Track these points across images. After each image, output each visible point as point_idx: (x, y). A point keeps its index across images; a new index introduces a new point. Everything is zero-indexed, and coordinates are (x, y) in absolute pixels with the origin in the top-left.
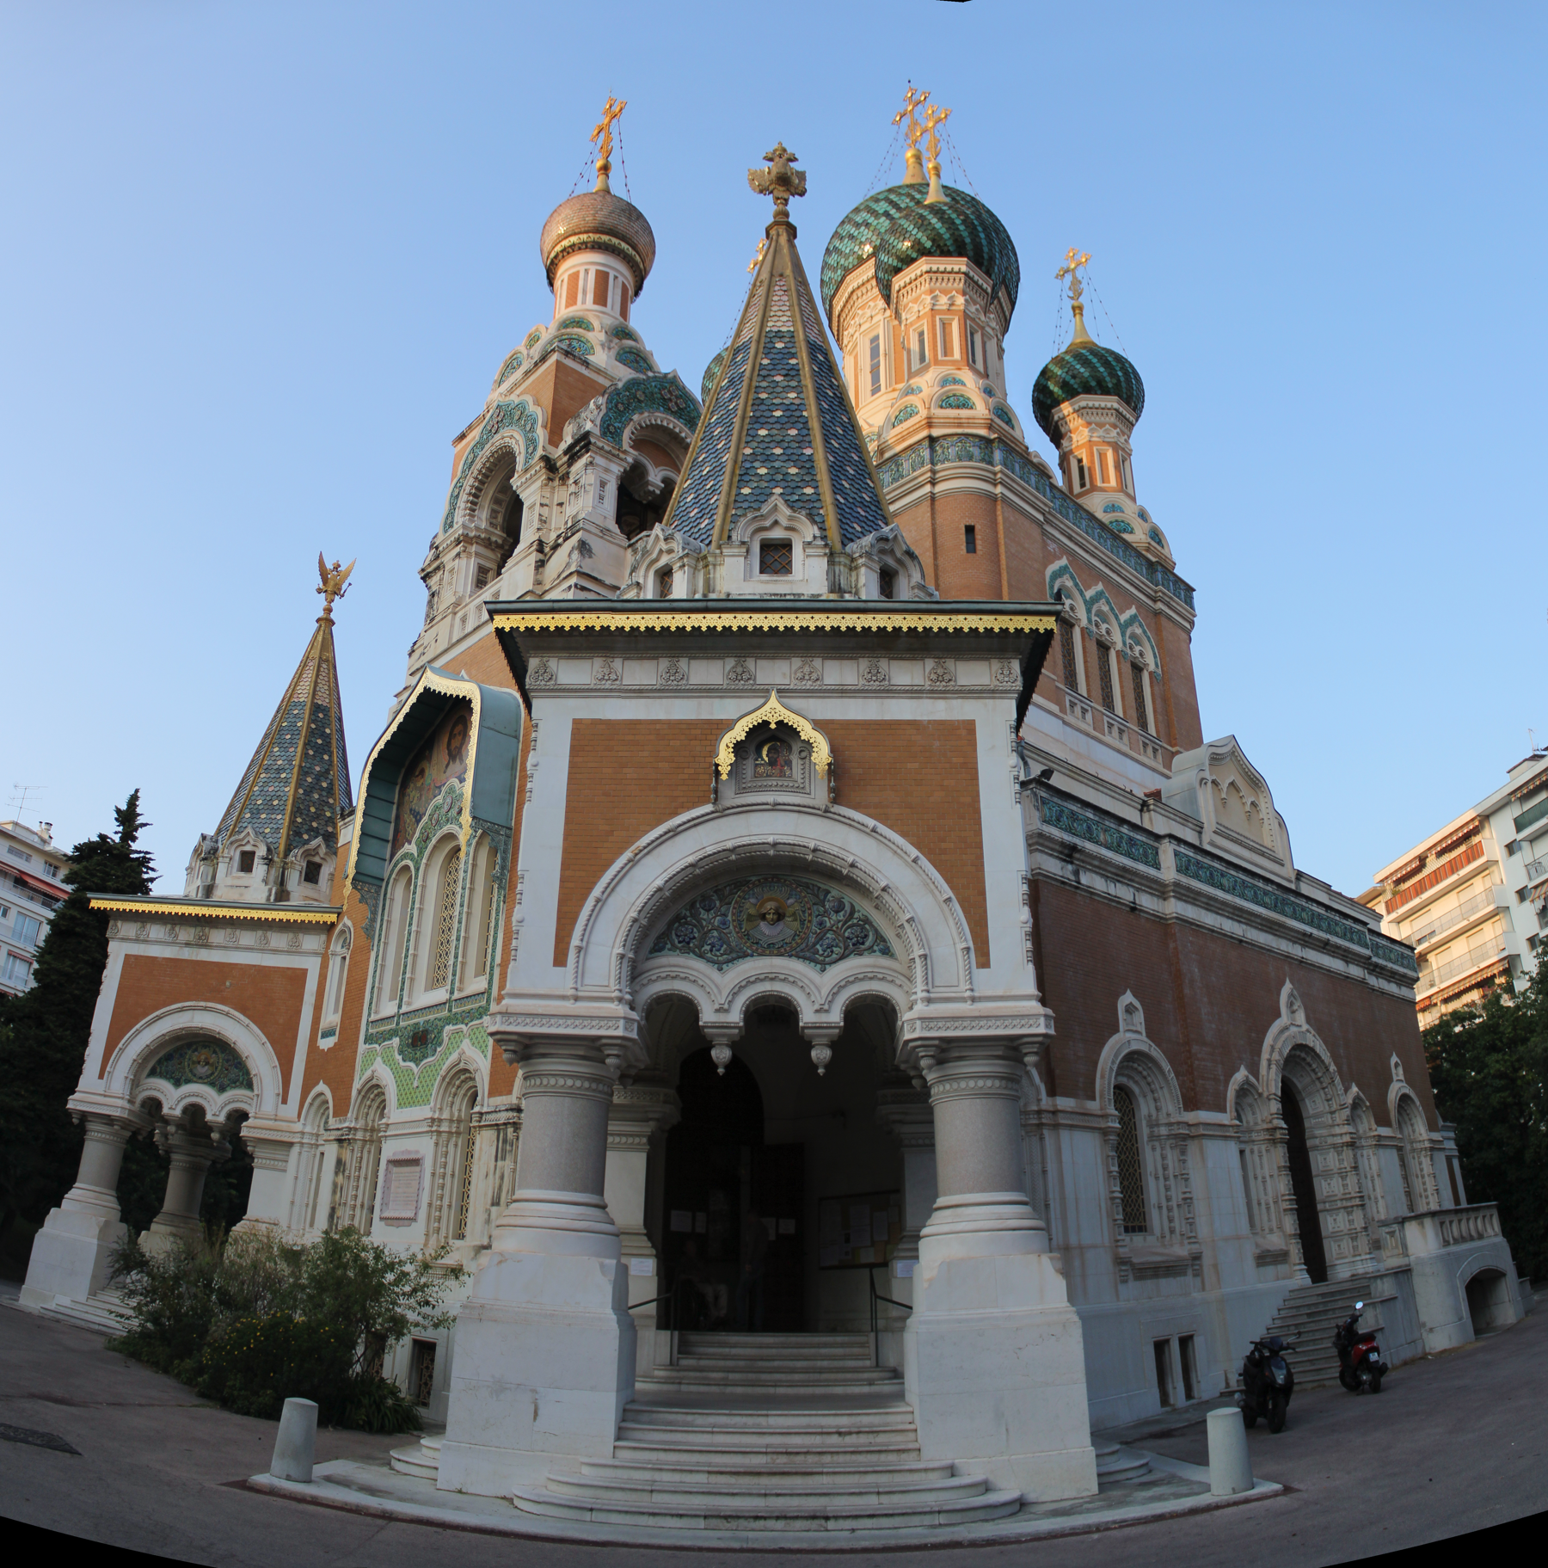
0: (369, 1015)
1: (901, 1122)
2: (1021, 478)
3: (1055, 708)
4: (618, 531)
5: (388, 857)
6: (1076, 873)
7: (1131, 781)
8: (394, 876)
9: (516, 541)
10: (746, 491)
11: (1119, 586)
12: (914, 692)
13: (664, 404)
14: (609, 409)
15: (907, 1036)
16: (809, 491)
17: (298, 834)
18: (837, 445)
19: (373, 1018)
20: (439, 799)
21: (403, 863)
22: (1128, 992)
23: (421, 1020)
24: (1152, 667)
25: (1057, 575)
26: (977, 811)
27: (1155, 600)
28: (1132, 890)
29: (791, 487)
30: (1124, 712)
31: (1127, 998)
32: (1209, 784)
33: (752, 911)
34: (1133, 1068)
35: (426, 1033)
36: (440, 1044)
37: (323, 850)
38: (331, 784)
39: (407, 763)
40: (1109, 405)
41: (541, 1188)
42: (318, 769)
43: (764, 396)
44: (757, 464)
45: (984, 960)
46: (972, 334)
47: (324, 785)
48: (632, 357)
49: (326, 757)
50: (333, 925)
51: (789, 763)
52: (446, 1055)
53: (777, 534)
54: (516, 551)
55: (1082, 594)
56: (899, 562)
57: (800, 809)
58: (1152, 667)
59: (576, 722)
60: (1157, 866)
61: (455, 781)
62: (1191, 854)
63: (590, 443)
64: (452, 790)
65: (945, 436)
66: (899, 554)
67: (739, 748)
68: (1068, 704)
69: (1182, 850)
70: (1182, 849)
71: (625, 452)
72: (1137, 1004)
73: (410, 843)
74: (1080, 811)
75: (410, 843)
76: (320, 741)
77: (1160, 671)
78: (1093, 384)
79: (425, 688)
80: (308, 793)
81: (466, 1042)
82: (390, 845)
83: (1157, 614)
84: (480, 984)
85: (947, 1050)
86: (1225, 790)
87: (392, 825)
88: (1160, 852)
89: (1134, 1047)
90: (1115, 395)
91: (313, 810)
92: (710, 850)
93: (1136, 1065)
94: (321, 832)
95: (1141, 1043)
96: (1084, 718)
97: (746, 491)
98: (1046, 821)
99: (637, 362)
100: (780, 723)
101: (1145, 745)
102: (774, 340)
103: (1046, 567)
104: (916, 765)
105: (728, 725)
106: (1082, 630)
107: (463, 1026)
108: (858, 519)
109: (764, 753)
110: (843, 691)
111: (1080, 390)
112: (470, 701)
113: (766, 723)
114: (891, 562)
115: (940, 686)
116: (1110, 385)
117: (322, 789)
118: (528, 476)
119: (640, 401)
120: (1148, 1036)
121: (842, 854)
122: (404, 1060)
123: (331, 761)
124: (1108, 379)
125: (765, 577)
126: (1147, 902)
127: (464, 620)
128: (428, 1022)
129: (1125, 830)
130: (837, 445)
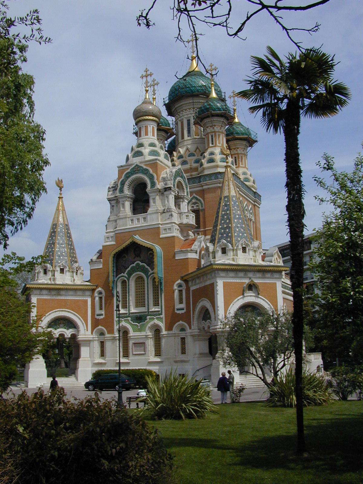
8: (119, 280)
20: (134, 265)
24: (253, 220)
27: (254, 202)
29: (243, 234)
42: (70, 243)
43: (234, 212)
49: (71, 239)
51: (252, 289)
58: (253, 220)
61: (140, 262)
73: (124, 273)
75: (124, 273)
79: (133, 241)
83: (255, 205)
97: (236, 234)
117: (72, 249)
125: (243, 254)
128: (141, 315)
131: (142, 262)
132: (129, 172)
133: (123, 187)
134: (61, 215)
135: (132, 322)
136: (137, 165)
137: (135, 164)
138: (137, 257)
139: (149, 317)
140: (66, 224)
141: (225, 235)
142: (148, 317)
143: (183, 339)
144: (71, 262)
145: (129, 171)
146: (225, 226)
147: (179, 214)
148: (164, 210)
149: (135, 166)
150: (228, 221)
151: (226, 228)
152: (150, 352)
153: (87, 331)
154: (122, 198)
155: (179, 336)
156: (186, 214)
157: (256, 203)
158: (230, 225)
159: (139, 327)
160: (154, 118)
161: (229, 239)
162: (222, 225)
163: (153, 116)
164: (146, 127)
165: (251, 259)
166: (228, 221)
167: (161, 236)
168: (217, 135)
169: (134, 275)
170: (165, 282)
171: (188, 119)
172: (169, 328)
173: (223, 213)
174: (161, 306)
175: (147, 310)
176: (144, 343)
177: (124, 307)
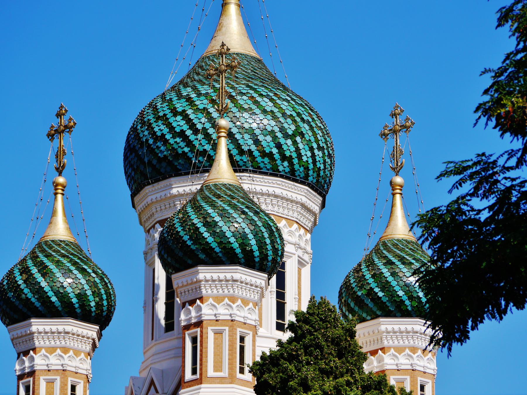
111: (379, 313)
116: (409, 308)
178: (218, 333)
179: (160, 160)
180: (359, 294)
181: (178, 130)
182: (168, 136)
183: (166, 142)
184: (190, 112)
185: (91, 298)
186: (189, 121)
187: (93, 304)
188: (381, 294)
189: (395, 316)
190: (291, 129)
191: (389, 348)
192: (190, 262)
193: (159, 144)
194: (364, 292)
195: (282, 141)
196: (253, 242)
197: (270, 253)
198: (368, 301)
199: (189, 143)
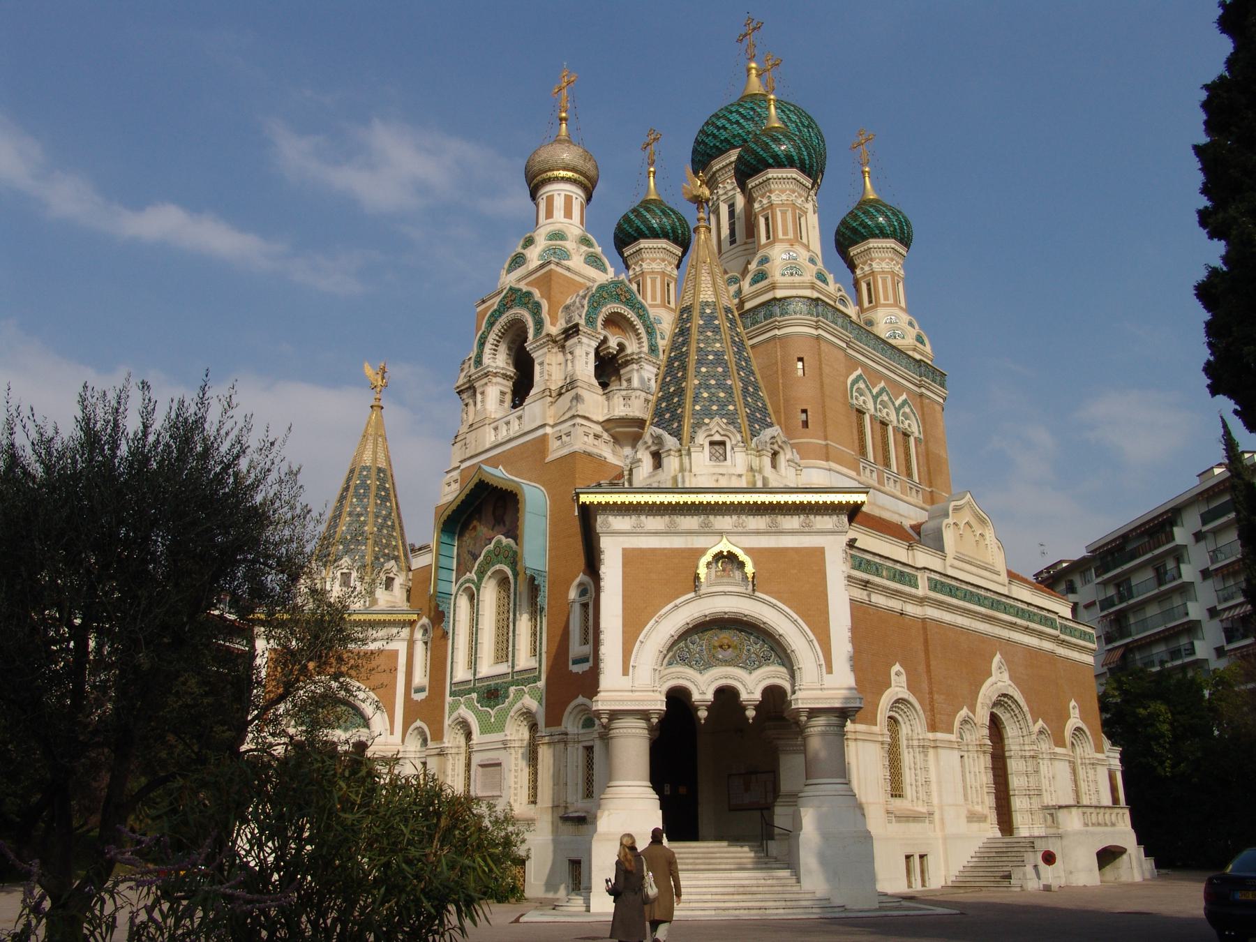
0: (451, 679)
1: (778, 739)
2: (832, 322)
3: (853, 474)
4: (597, 384)
5: (454, 580)
6: (869, 596)
7: (901, 515)
8: (460, 593)
9: (531, 386)
10: (698, 408)
11: (896, 381)
12: (793, 532)
13: (617, 298)
14: (589, 307)
15: (793, 707)
16: (731, 407)
17: (377, 558)
18: (743, 375)
19: (455, 680)
20: (491, 546)
21: (467, 585)
22: (897, 664)
23: (492, 683)
24: (917, 434)
25: (854, 383)
26: (826, 595)
28: (901, 602)
29: (723, 406)
30: (898, 469)
31: (897, 667)
32: (952, 527)
33: (716, 644)
34: (899, 708)
35: (496, 690)
36: (508, 697)
37: (395, 569)
38: (393, 522)
39: (462, 520)
40: (888, 245)
41: (639, 780)
42: (384, 512)
43: (702, 345)
44: (702, 390)
45: (830, 671)
46: (799, 219)
47: (389, 523)
48: (593, 259)
49: (388, 504)
50: (414, 621)
52: (512, 704)
53: (717, 438)
54: (532, 392)
55: (871, 392)
56: (780, 447)
57: (739, 594)
58: (917, 434)
59: (624, 549)
60: (916, 587)
61: (503, 538)
62: (938, 578)
63: (579, 330)
64: (499, 542)
65: (785, 298)
66: (780, 443)
67: (709, 564)
68: (861, 468)
69: (933, 576)
70: (933, 576)
71: (599, 333)
72: (902, 670)
73: (471, 573)
74: (872, 559)
75: (471, 573)
76: (383, 493)
77: (922, 437)
78: (877, 232)
79: (480, 480)
80: (380, 530)
81: (527, 696)
82: (454, 572)
83: (921, 395)
84: (533, 663)
85: (813, 713)
86: (962, 528)
87: (455, 560)
88: (919, 578)
89: (900, 696)
90: (893, 238)
91: (384, 541)
92: (696, 615)
93: (900, 705)
94: (391, 556)
95: (905, 694)
96: (871, 476)
97: (698, 408)
98: (854, 568)
99: (596, 262)
100: (729, 552)
101: (911, 488)
102: (704, 307)
103: (848, 377)
104: (795, 571)
105: (703, 552)
106: (871, 416)
107: (523, 687)
108: (757, 421)
109: (720, 565)
110: (758, 533)
112: (516, 495)
113: (721, 552)
114: (776, 447)
115: (807, 529)
116: (889, 232)
117: (388, 526)
118: (534, 345)
119: (605, 299)
120: (908, 689)
121: (760, 617)
122: (482, 706)
123: (391, 506)
124: (887, 228)
125: (713, 463)
126: (911, 609)
127: (496, 429)
128: (497, 684)
129: (898, 567)
130: (743, 375)
131: (507, 537)
132: (495, 311)
133: (482, 352)
134: (370, 446)
135: (479, 705)
136: (511, 289)
137: (508, 287)
138: (499, 524)
139: (514, 687)
140: (380, 470)
141: (667, 416)
142: (512, 689)
143: (589, 749)
144: (377, 558)
145: (495, 307)
146: (671, 390)
147: (605, 396)
148: (562, 387)
149: (507, 293)
150: (680, 374)
151: (674, 393)
152: (512, 791)
153: (392, 733)
154: (479, 378)
155: (579, 742)
156: (624, 393)
157: (923, 390)
158: (683, 385)
159: (493, 720)
160: (570, 174)
161: (675, 425)
162: (665, 388)
163: (565, 169)
164: (550, 200)
165: (740, 476)
166: (680, 374)
167: (550, 458)
168: (779, 214)
169: (489, 573)
170: (552, 584)
171: (731, 202)
172: (554, 716)
173: (672, 354)
174: (540, 654)
175: (510, 670)
176: (499, 765)
177: (473, 663)
178: (784, 213)
179: (722, 142)
180: (854, 225)
181: (734, 121)
182: (728, 126)
183: (725, 128)
184: (741, 110)
185: (679, 227)
186: (740, 114)
187: (680, 232)
188: (870, 223)
189: (879, 237)
190: (806, 123)
191: (875, 259)
192: (761, 168)
193: (721, 131)
194: (858, 223)
195: (801, 128)
196: (805, 153)
197: (815, 164)
198: (860, 228)
199: (742, 127)
